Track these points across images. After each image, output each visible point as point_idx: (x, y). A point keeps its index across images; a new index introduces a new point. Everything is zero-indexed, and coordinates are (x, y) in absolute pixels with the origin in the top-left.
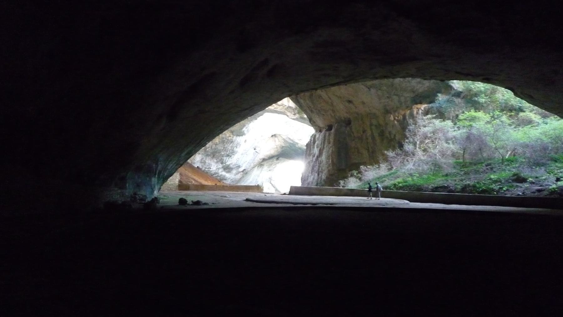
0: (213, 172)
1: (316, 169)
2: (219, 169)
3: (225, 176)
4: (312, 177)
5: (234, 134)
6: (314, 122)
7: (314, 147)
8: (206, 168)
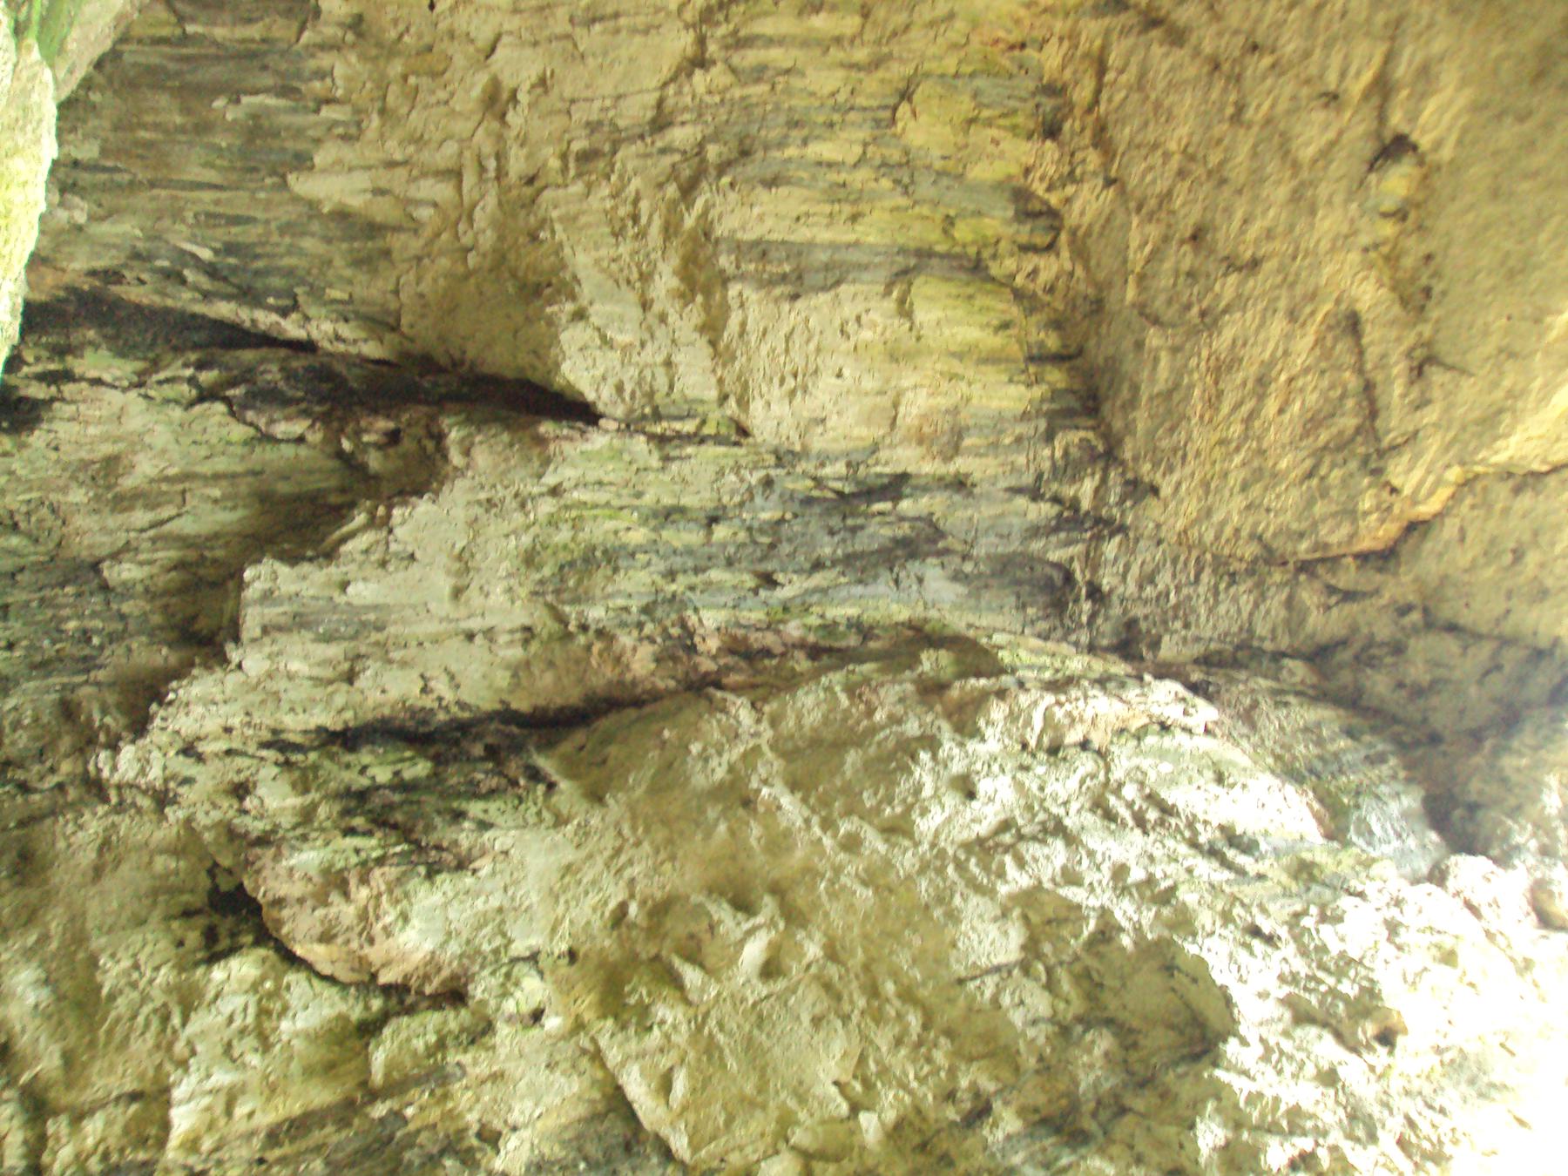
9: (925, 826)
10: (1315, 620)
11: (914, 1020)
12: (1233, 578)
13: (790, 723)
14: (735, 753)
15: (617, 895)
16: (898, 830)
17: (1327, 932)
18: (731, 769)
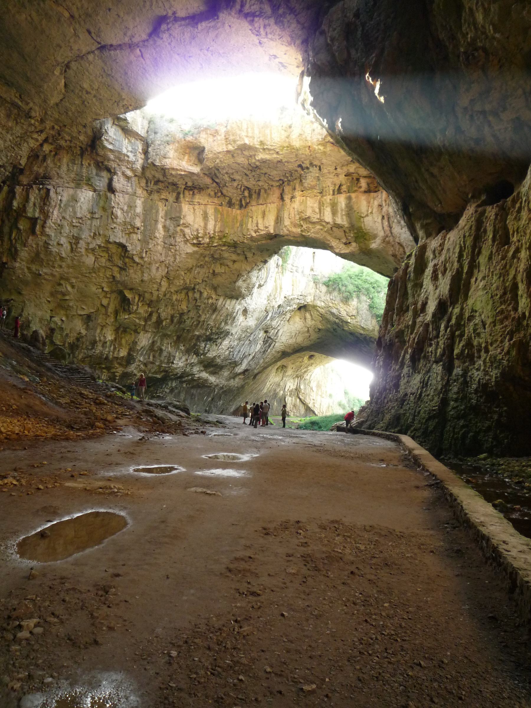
0: (179, 371)
1: (436, 349)
2: (192, 365)
3: (206, 380)
4: (417, 379)
5: (219, 291)
6: (422, 205)
7: (419, 285)
8: (161, 362)
9: (64, 255)
10: (40, 138)
11: (94, 275)
12: (20, 144)
13: (24, 259)
14: (26, 270)
15: (44, 300)
16: (62, 258)
17: (118, 220)
18: (30, 273)
